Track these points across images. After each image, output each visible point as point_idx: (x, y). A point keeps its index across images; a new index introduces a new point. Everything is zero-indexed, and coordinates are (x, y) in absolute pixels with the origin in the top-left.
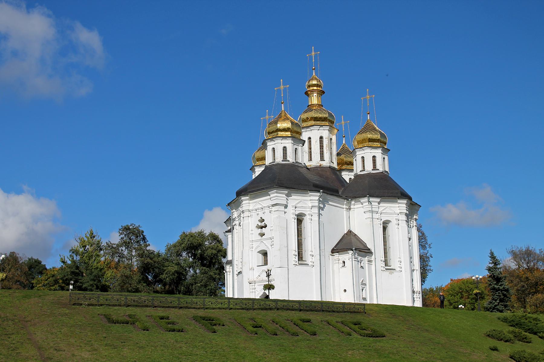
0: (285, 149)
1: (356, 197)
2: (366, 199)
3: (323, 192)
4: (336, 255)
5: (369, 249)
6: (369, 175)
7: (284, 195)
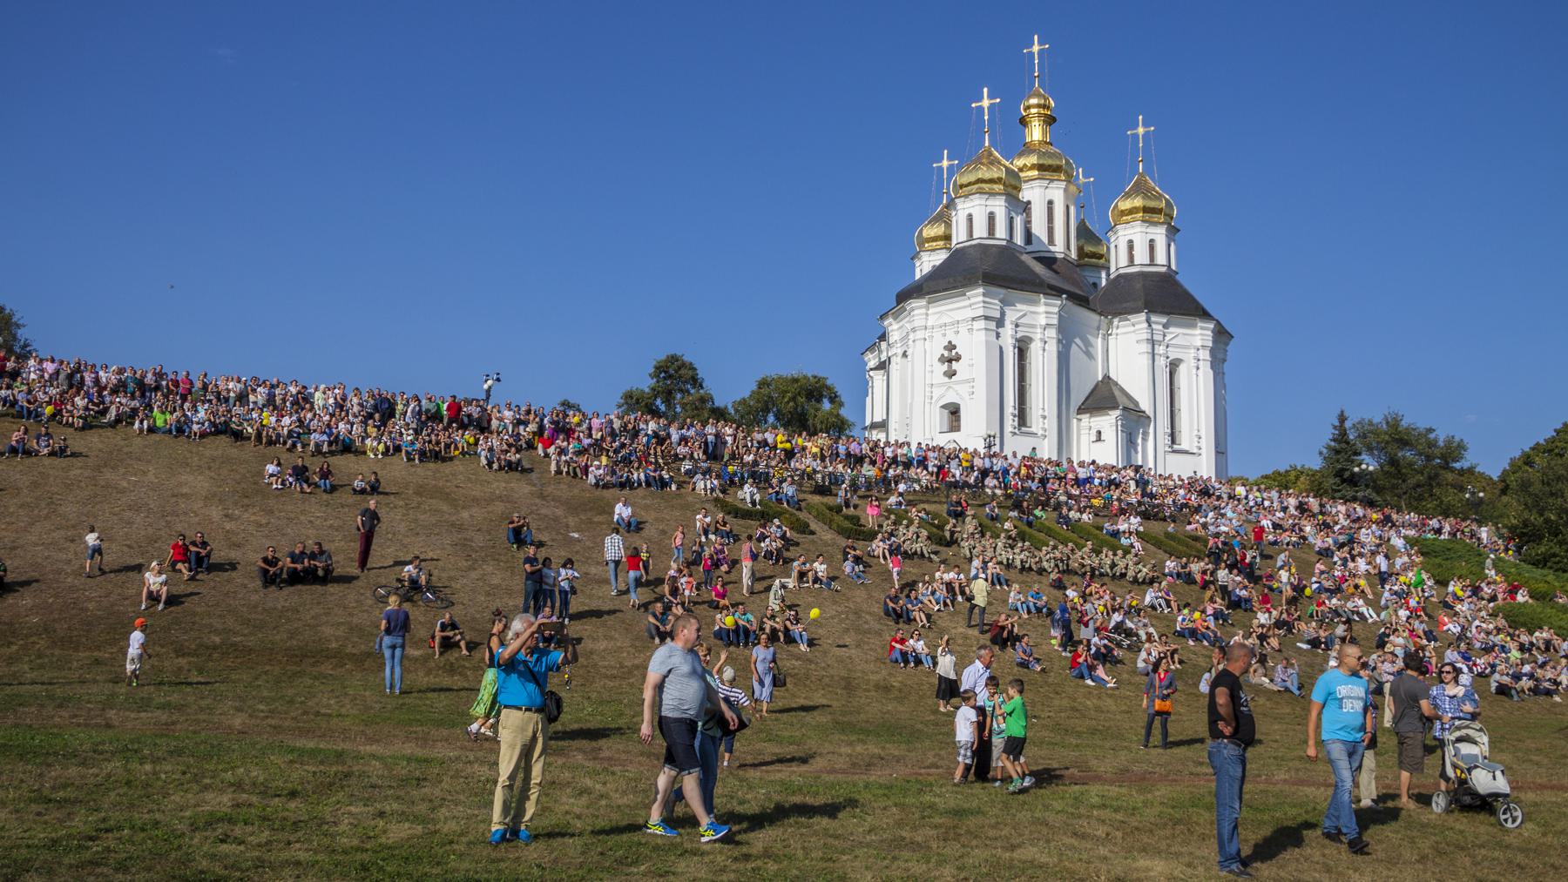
0: (991, 218)
1: (1120, 314)
2: (1142, 317)
3: (1066, 299)
4: (1085, 418)
5: (1144, 412)
6: (1143, 276)
7: (997, 302)
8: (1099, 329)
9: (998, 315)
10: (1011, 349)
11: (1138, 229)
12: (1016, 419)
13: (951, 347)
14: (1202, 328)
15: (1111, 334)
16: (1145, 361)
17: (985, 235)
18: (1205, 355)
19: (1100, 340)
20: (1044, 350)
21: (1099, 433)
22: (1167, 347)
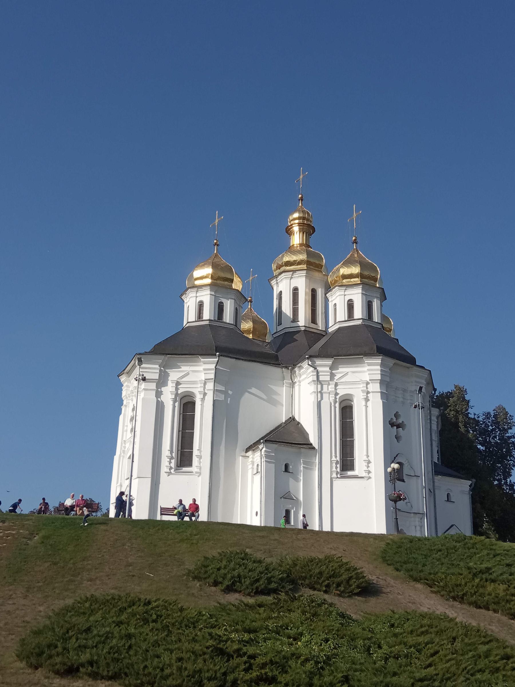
5: (311, 444)
8: (284, 378)
9: (156, 376)
10: (171, 403)
11: (338, 293)
14: (369, 365)
15: (295, 382)
18: (376, 387)
22: (336, 385)
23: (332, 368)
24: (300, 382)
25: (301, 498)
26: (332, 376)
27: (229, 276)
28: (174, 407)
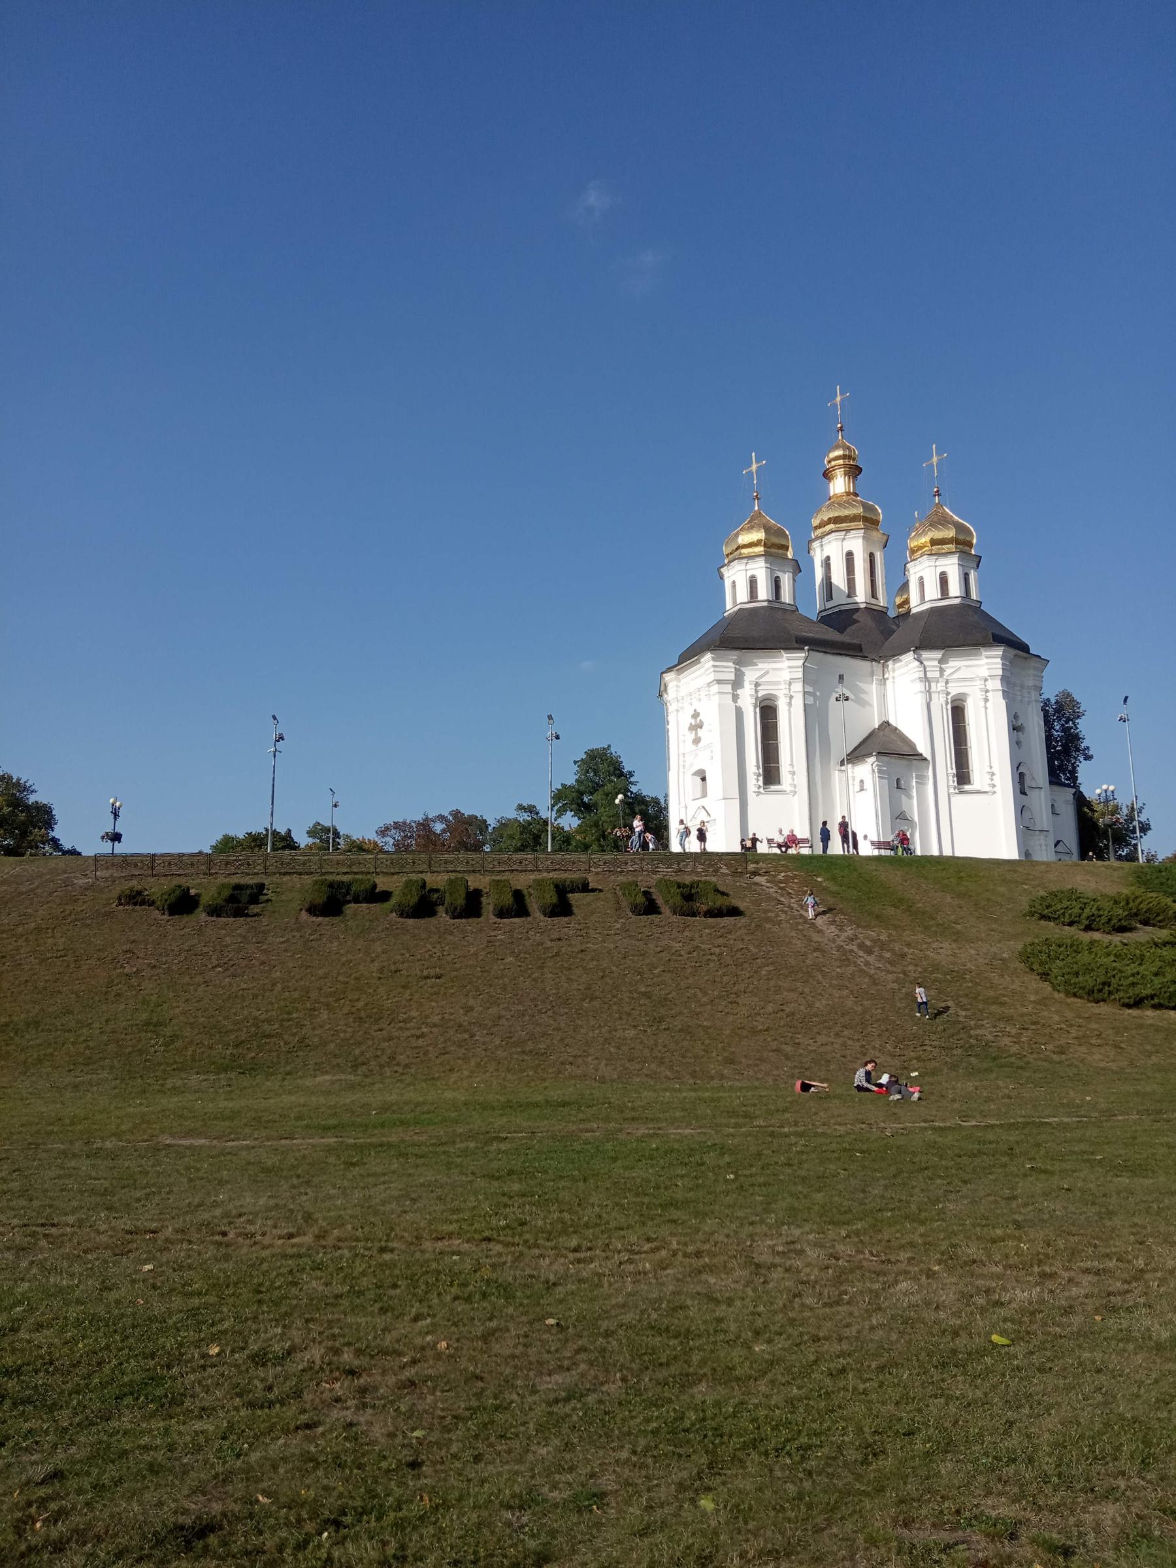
2: (909, 657)
5: (921, 755)
7: (731, 664)
8: (872, 674)
9: (732, 677)
10: (752, 709)
12: (761, 778)
13: (696, 715)
14: (988, 657)
15: (888, 679)
16: (919, 701)
17: (746, 600)
18: (996, 684)
19: (874, 685)
20: (790, 704)
21: (862, 781)
22: (947, 682)
23: (941, 661)
24: (894, 678)
25: (916, 819)
26: (942, 671)
27: (783, 542)
28: (755, 713)
